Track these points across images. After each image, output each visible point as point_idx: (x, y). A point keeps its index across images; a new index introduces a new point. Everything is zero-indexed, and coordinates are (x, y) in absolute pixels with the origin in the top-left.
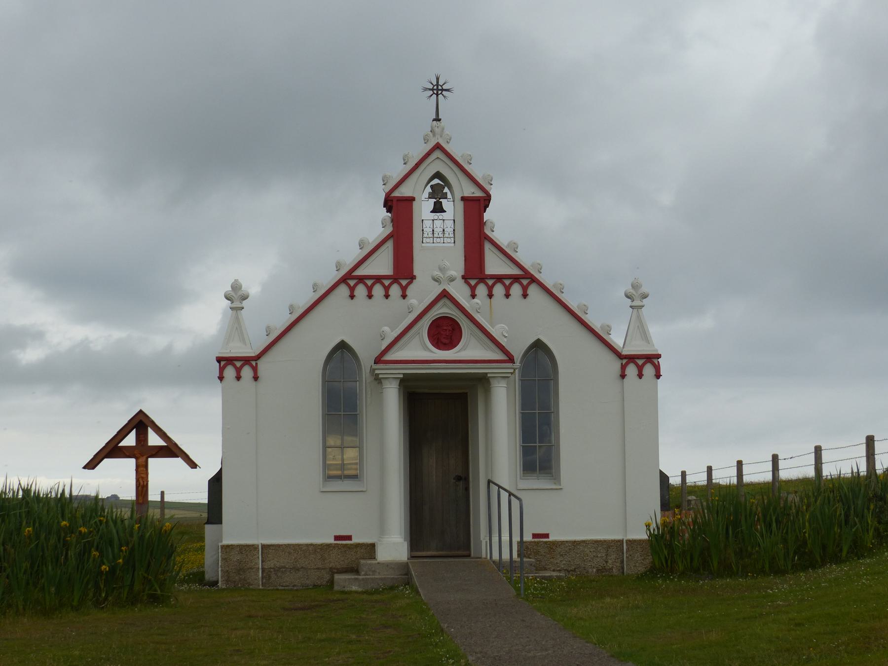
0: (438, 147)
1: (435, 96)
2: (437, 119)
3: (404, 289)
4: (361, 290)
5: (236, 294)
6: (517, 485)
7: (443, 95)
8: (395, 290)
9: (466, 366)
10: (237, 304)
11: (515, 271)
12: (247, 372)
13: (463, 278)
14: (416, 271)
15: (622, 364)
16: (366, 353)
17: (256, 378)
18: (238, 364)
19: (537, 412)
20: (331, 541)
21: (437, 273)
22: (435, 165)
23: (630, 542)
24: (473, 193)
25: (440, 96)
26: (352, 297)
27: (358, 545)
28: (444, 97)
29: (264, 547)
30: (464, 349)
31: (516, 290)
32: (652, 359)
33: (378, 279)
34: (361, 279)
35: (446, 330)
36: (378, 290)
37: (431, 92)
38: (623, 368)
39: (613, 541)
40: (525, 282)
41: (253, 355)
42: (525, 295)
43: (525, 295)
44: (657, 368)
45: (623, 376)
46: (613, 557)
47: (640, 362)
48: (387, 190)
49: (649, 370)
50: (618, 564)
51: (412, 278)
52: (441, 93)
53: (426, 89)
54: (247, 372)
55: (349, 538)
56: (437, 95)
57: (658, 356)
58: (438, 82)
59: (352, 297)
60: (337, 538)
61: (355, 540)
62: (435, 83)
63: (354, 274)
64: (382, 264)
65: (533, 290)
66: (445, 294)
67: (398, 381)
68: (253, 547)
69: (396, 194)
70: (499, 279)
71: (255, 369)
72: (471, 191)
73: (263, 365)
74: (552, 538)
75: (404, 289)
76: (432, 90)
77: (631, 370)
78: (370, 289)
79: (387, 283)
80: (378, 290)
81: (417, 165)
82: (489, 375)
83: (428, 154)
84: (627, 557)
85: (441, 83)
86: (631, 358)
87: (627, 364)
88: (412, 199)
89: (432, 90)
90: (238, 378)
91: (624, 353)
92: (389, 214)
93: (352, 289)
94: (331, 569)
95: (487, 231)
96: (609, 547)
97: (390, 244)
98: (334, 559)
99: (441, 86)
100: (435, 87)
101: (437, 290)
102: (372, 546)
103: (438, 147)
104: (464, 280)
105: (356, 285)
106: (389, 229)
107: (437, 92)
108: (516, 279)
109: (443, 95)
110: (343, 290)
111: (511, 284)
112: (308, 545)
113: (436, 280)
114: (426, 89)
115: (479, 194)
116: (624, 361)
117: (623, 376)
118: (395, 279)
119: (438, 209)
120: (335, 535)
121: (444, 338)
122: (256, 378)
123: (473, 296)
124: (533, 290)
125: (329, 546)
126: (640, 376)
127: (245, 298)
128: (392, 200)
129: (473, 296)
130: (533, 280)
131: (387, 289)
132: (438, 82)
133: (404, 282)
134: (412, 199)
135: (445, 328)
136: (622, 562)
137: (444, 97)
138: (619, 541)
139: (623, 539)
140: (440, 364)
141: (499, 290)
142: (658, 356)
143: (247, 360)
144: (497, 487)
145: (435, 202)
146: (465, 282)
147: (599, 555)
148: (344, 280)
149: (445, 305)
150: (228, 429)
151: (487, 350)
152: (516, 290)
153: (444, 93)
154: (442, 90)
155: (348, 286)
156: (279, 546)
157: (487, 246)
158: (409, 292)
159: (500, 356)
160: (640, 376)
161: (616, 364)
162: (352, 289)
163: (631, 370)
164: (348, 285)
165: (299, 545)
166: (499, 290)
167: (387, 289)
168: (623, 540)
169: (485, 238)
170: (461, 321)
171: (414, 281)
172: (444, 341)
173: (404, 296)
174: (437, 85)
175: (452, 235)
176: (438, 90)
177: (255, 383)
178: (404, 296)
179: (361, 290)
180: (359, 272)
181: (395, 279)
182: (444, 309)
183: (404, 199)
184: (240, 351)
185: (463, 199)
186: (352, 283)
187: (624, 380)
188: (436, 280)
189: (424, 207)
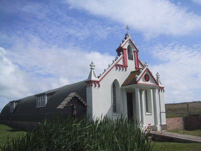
6: (146, 113)
12: (97, 85)
17: (99, 86)
26: (117, 69)
32: (163, 88)
33: (122, 66)
34: (119, 65)
51: (127, 66)
54: (97, 85)
74: (151, 125)
77: (160, 90)
86: (160, 88)
88: (126, 49)
110: (115, 68)
117: (159, 91)
127: (94, 66)
143: (98, 82)
159: (156, 84)
173: (126, 70)
179: (118, 68)
185: (134, 51)
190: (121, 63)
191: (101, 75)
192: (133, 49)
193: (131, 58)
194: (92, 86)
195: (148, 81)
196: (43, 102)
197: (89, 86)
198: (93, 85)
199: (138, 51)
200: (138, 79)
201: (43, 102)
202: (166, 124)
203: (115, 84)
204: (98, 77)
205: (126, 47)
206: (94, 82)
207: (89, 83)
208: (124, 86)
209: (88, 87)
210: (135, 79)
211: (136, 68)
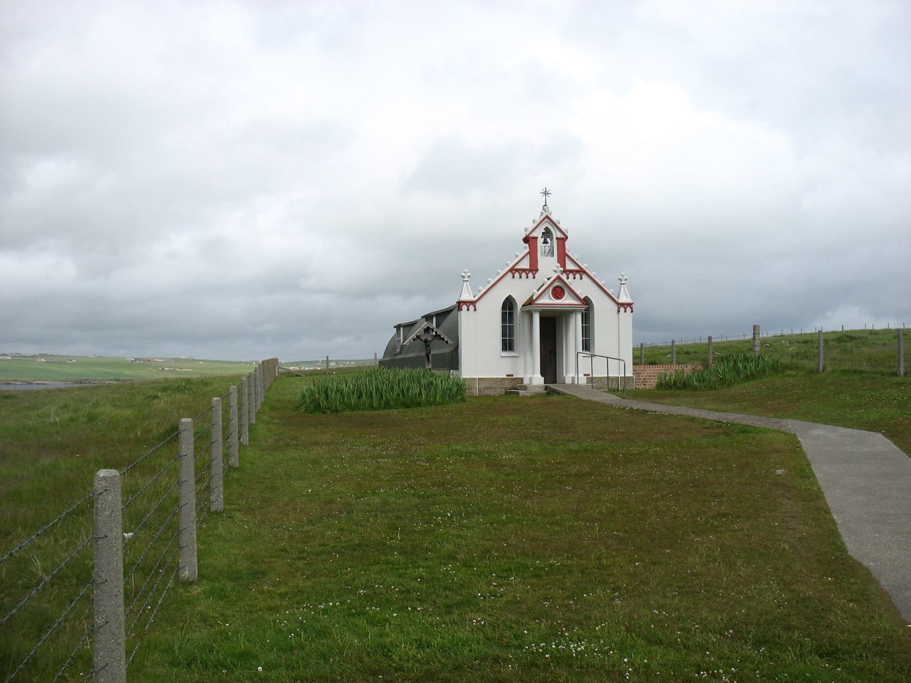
0: (547, 217)
2: (546, 205)
4: (517, 275)
8: (530, 275)
11: (577, 268)
12: (472, 307)
14: (538, 268)
16: (520, 301)
17: (475, 310)
20: (505, 377)
21: (555, 268)
23: (621, 378)
25: (547, 196)
26: (513, 277)
27: (516, 378)
28: (549, 196)
29: (478, 379)
30: (565, 300)
31: (578, 276)
32: (630, 305)
33: (524, 270)
34: (518, 270)
36: (524, 275)
39: (615, 377)
40: (581, 273)
42: (581, 278)
43: (581, 278)
44: (632, 309)
45: (619, 311)
46: (615, 383)
48: (527, 234)
49: (629, 309)
51: (537, 270)
53: (541, 193)
54: (472, 307)
55: (512, 375)
57: (633, 304)
59: (513, 277)
60: (507, 375)
61: (514, 377)
64: (525, 264)
65: (584, 276)
66: (559, 278)
68: (475, 379)
69: (531, 236)
70: (571, 271)
72: (560, 235)
73: (477, 305)
76: (544, 193)
77: (622, 309)
78: (520, 275)
80: (524, 275)
81: (539, 224)
83: (543, 220)
85: (547, 190)
86: (622, 305)
87: (620, 307)
88: (536, 238)
89: (544, 193)
90: (468, 310)
91: (620, 302)
92: (527, 245)
93: (513, 274)
94: (505, 388)
95: (567, 252)
97: (528, 256)
98: (507, 385)
101: (554, 276)
102: (522, 379)
103: (547, 217)
105: (515, 273)
106: (528, 250)
108: (577, 272)
110: (510, 275)
111: (576, 274)
112: (496, 378)
113: (555, 271)
114: (541, 193)
115: (563, 236)
117: (619, 311)
118: (530, 270)
119: (545, 242)
120: (508, 374)
122: (475, 310)
123: (568, 278)
124: (584, 276)
125: (504, 378)
126: (625, 311)
129: (568, 278)
130: (584, 272)
134: (536, 238)
137: (549, 196)
141: (571, 276)
142: (633, 304)
143: (473, 303)
144: (606, 358)
149: (558, 282)
152: (578, 276)
154: (548, 193)
156: (484, 378)
157: (567, 258)
158: (535, 276)
160: (625, 311)
161: (615, 307)
162: (513, 274)
163: (622, 309)
165: (493, 378)
166: (571, 276)
167: (527, 275)
173: (534, 278)
177: (474, 312)
178: (534, 278)
179: (517, 275)
180: (516, 267)
181: (530, 270)
182: (557, 284)
185: (557, 238)
187: (620, 313)
188: (555, 271)
189: (540, 241)
190: (525, 264)
192: (556, 234)
198: (464, 307)
199: (567, 238)
202: (632, 375)
203: (509, 305)
205: (538, 234)
206: (465, 302)
208: (526, 307)
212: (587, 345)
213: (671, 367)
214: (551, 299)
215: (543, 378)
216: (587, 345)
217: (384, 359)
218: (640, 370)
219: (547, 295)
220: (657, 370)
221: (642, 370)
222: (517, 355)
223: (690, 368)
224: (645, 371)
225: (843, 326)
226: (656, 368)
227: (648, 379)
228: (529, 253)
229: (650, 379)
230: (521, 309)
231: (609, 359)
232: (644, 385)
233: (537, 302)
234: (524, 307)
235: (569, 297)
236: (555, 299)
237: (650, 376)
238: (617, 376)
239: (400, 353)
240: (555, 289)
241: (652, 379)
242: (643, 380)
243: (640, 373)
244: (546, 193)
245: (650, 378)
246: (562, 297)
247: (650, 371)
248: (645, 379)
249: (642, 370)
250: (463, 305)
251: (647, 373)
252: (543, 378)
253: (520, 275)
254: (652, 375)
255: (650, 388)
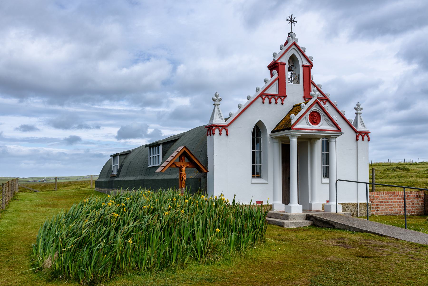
1: (291, 23)
3: (282, 101)
4: (267, 100)
5: (217, 98)
6: (322, 181)
7: (294, 23)
8: (279, 101)
9: (325, 132)
10: (217, 103)
12: (224, 132)
13: (303, 98)
15: (357, 135)
17: (227, 135)
18: (221, 128)
19: (325, 152)
22: (292, 51)
24: (307, 64)
25: (293, 23)
26: (263, 102)
28: (294, 24)
32: (367, 133)
33: (273, 96)
34: (267, 95)
35: (316, 117)
36: (273, 100)
37: (289, 22)
38: (357, 137)
39: (354, 203)
40: (325, 101)
41: (227, 125)
45: (357, 140)
46: (354, 210)
47: (363, 135)
48: (276, 60)
49: (366, 138)
50: (355, 213)
51: (285, 96)
52: (293, 22)
53: (288, 20)
54: (224, 132)
56: (292, 23)
57: (370, 132)
58: (292, 18)
59: (263, 102)
62: (291, 18)
63: (265, 93)
64: (274, 90)
67: (297, 137)
69: (279, 61)
71: (227, 131)
72: (306, 63)
73: (229, 129)
75: (282, 101)
77: (360, 137)
78: (270, 100)
79: (276, 98)
80: (273, 100)
82: (332, 136)
84: (359, 210)
86: (360, 133)
87: (359, 135)
88: (284, 64)
89: (290, 20)
93: (263, 99)
96: (353, 206)
97: (277, 82)
99: (293, 19)
100: (291, 20)
104: (303, 99)
107: (292, 22)
109: (294, 23)
110: (260, 99)
114: (288, 20)
115: (308, 64)
116: (358, 134)
117: (357, 140)
121: (315, 120)
122: (227, 135)
126: (363, 140)
127: (220, 100)
128: (278, 64)
130: (328, 100)
131: (276, 100)
132: (292, 18)
133: (283, 98)
135: (316, 116)
136: (357, 211)
137: (294, 24)
138: (356, 204)
139: (357, 203)
140: (316, 131)
142: (370, 132)
143: (224, 127)
145: (289, 67)
146: (304, 99)
147: (349, 209)
148: (261, 95)
149: (316, 106)
150: (216, 156)
151: (330, 126)
153: (294, 22)
154: (293, 21)
155: (262, 98)
157: (312, 86)
158: (285, 102)
159: (335, 129)
160: (363, 140)
161: (354, 135)
162: (263, 99)
163: (360, 137)
164: (262, 98)
167: (276, 100)
168: (357, 203)
169: (312, 83)
170: (322, 114)
171: (286, 98)
172: (315, 121)
173: (282, 104)
174: (292, 19)
175: (298, 80)
176: (292, 21)
178: (282, 104)
179: (267, 100)
180: (266, 92)
181: (279, 97)
183: (283, 63)
184: (219, 122)
185: (303, 66)
186: (264, 97)
187: (358, 141)
191: (231, 115)
192: (302, 62)
193: (296, 80)
194: (214, 134)
195: (318, 124)
196: (157, 157)
197: (210, 135)
198: (217, 131)
199: (312, 65)
200: (293, 122)
201: (157, 157)
204: (226, 120)
205: (285, 60)
206: (217, 126)
207: (210, 129)
209: (209, 135)
210: (290, 120)
211: (304, 98)
212: (326, 174)
213: (398, 194)
214: (308, 124)
215: (302, 206)
216: (326, 174)
217: (100, 180)
218: (373, 197)
219: (304, 120)
220: (387, 196)
221: (375, 197)
222: (266, 182)
223: (414, 195)
224: (378, 197)
225: (419, 159)
226: (387, 195)
227: (380, 205)
228: (278, 79)
229: (382, 205)
230: (270, 135)
231: (328, 185)
232: (378, 211)
233: (297, 126)
234: (273, 134)
235: (325, 123)
236: (313, 124)
237: (382, 202)
238: (356, 202)
239: (118, 176)
240: (312, 114)
241: (384, 205)
242: (376, 206)
243: (373, 199)
244: (292, 21)
245: (381, 204)
246: (318, 122)
247: (381, 197)
248: (377, 205)
249: (375, 197)
250: (215, 129)
251: (380, 199)
252: (302, 206)
253: (270, 100)
254: (383, 201)
255: (382, 213)
